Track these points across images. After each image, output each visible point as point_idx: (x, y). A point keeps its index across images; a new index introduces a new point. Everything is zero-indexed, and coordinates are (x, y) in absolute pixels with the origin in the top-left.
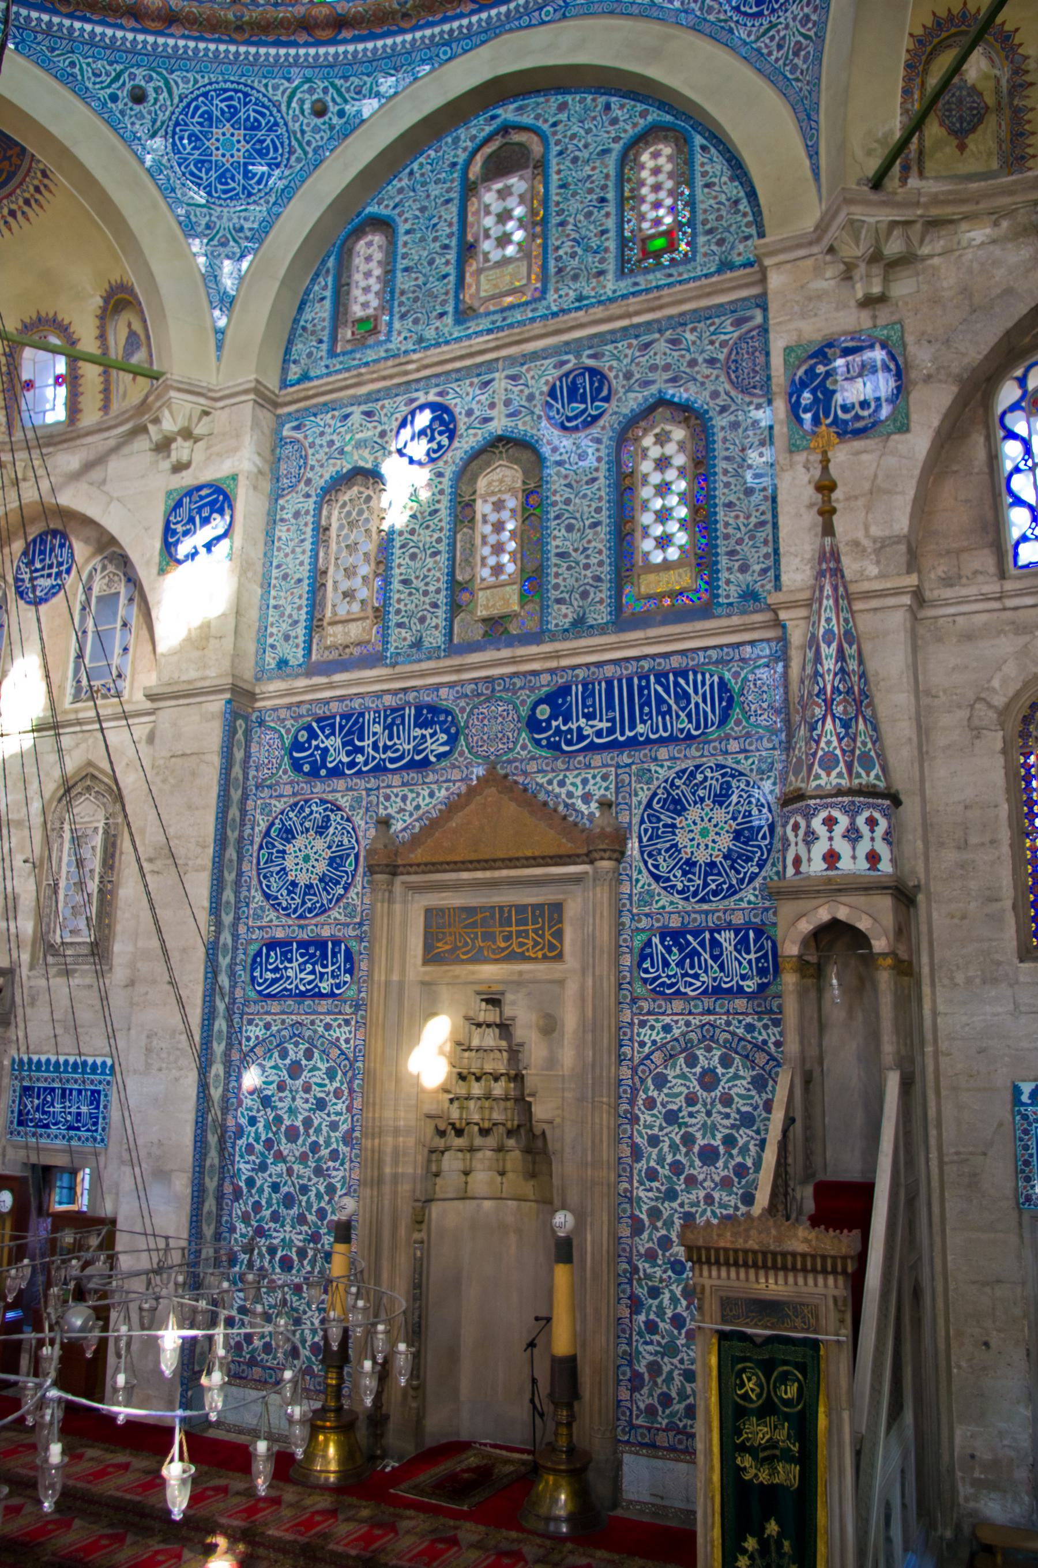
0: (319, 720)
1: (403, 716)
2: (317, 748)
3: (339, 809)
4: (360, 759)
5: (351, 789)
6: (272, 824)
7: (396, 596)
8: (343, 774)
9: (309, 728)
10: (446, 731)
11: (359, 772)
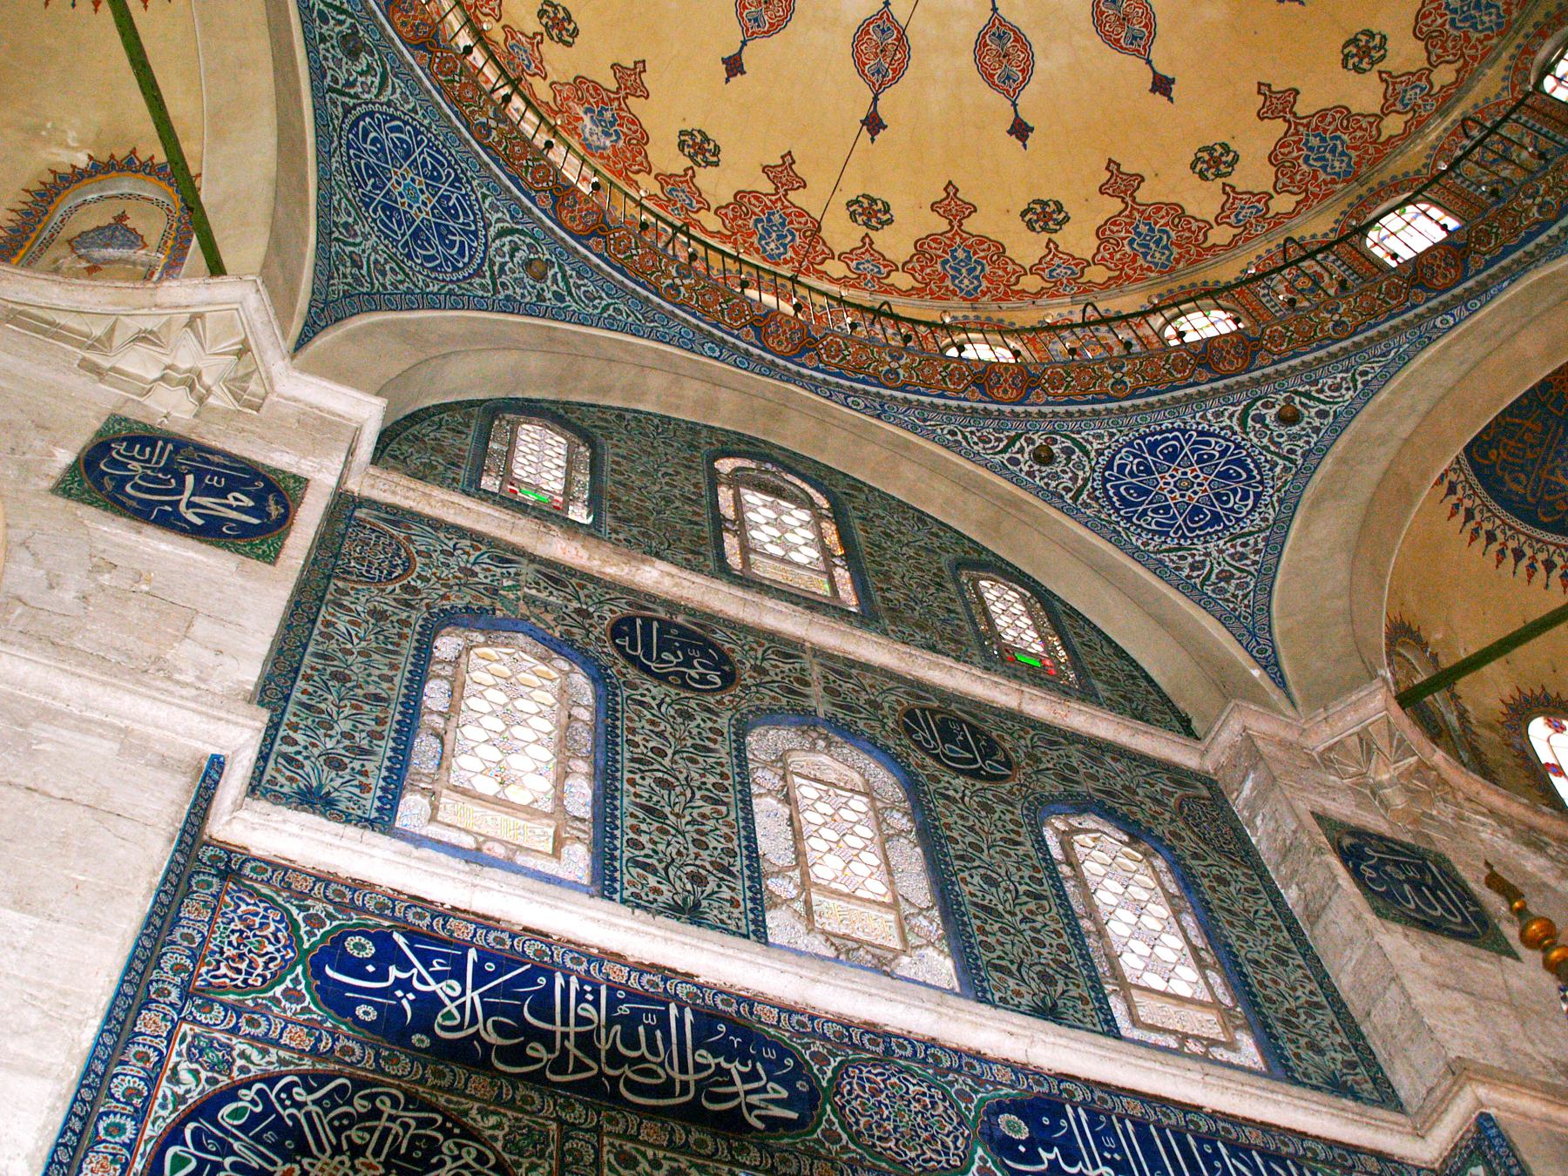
0: (413, 936)
1: (664, 1017)
2: (405, 985)
3: (471, 1134)
4: (536, 1050)
5: (511, 1104)
6: (230, 1094)
7: (629, 821)
8: (484, 1065)
9: (382, 939)
10: (786, 1081)
11: (537, 1079)
